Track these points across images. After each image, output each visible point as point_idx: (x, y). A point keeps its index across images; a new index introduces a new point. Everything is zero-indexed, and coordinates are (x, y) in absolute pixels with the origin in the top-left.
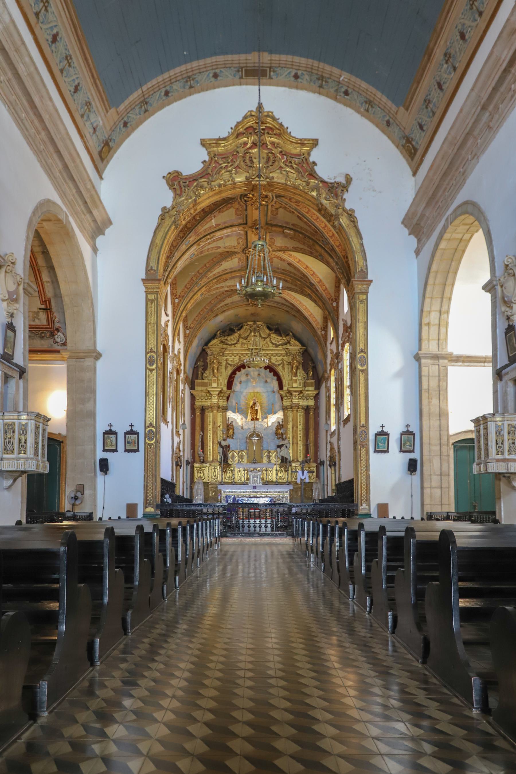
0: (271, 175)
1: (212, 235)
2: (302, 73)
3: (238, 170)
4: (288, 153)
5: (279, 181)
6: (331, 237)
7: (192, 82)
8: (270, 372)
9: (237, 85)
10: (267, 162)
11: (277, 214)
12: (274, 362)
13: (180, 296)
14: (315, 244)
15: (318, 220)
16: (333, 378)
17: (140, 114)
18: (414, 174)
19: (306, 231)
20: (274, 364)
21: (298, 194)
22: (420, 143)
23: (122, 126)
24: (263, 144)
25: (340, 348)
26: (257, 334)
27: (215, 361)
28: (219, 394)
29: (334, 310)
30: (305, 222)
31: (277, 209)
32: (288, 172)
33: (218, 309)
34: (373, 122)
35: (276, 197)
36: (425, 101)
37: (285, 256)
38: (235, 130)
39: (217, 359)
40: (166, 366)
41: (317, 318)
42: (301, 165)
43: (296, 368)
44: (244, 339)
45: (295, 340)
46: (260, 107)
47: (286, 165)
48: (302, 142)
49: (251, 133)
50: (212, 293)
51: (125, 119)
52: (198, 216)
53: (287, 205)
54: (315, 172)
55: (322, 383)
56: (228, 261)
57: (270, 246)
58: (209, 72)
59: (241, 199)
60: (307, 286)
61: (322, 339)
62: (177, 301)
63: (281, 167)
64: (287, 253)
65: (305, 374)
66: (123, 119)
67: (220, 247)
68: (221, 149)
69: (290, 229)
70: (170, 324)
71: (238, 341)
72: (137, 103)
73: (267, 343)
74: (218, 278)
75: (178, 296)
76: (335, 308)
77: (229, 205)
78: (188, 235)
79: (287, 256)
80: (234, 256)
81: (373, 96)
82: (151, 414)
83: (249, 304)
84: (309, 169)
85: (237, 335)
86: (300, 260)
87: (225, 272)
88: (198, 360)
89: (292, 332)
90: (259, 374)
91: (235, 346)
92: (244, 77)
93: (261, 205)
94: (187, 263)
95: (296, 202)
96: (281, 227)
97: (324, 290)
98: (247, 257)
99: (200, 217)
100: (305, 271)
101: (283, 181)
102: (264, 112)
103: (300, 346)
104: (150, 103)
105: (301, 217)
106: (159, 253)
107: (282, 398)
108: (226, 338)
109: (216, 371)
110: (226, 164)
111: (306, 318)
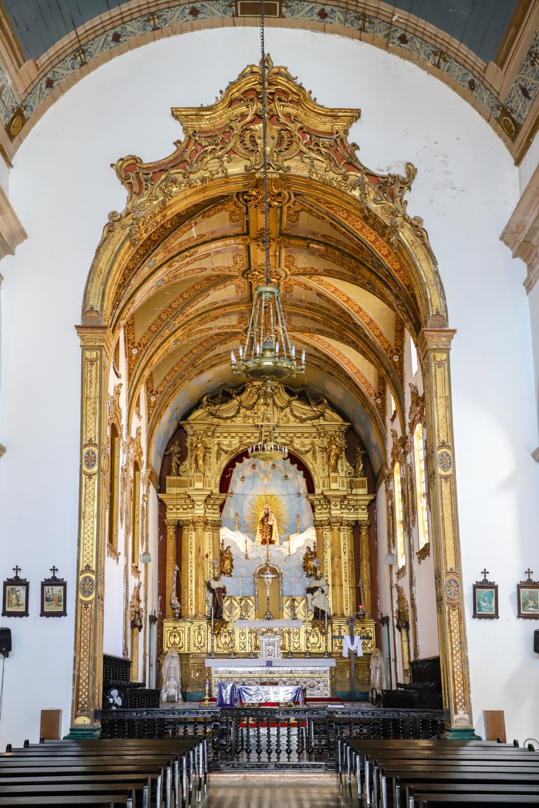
0: (286, 164)
1: (192, 251)
2: (332, 9)
3: (232, 156)
4: (313, 130)
5: (298, 173)
7: (157, 21)
8: (292, 463)
9: (229, 25)
10: (279, 144)
11: (297, 219)
12: (298, 446)
13: (139, 344)
14: (360, 266)
16: (397, 477)
17: (74, 69)
18: (518, 162)
19: (346, 246)
20: (298, 450)
21: (330, 194)
22: (524, 116)
23: (44, 86)
24: (272, 116)
25: (408, 429)
26: (270, 401)
27: (199, 446)
28: (206, 501)
29: (396, 368)
30: (344, 234)
32: (312, 160)
33: (204, 362)
34: (447, 83)
35: (295, 195)
36: (530, 54)
37: (312, 282)
38: (227, 95)
39: (203, 442)
40: (116, 458)
41: (368, 378)
42: (335, 148)
43: (335, 458)
44: (247, 409)
45: (333, 411)
46: (265, 60)
47: (309, 148)
48: (335, 114)
49: (252, 100)
50: (194, 338)
51: (50, 76)
53: (313, 207)
54: (357, 159)
55: (380, 484)
56: (219, 289)
57: (286, 267)
58: (183, 6)
59: (238, 198)
60: (350, 329)
61: (377, 412)
62: (135, 351)
63: (301, 151)
64: (314, 278)
65: (351, 468)
66: (45, 76)
67: (206, 269)
68: (204, 124)
69: (319, 242)
70: (124, 391)
71: (238, 412)
72: (68, 52)
73: (286, 416)
74: (203, 316)
75: (136, 345)
76: (397, 365)
77: (220, 207)
78: (153, 252)
79: (315, 283)
80: (229, 283)
81: (446, 44)
82: (88, 550)
84: (347, 156)
85: (235, 402)
86: (336, 289)
87: (214, 306)
88: (171, 443)
89: (326, 398)
90: (274, 465)
91: (232, 421)
92: (239, 15)
93: (270, 206)
94: (151, 293)
96: (304, 239)
97: (377, 336)
98: (251, 282)
100: (345, 306)
101: (305, 174)
102: (273, 67)
103: (340, 421)
104: (91, 52)
105: (335, 225)
106: (105, 284)
107: (313, 507)
108: (217, 407)
109: (200, 462)
110: (213, 147)
111: (349, 378)
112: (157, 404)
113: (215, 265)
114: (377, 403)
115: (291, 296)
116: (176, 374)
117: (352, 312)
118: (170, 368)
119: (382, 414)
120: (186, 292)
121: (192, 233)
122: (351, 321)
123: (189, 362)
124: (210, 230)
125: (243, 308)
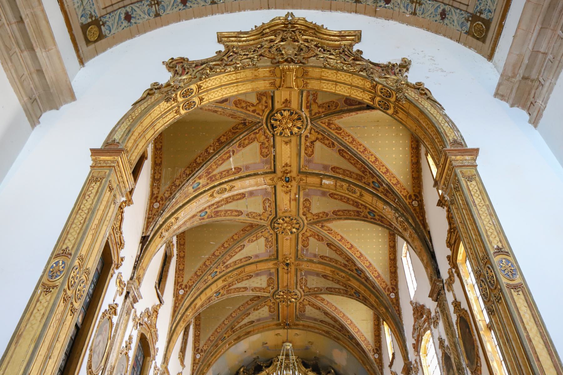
6: (385, 173)
15: (366, 153)
29: (393, 304)
31: (312, 143)
52: (212, 148)
56: (252, 241)
60: (354, 277)
61: (376, 365)
69: (329, 177)
74: (240, 270)
76: (395, 301)
79: (326, 232)
83: (280, 324)
86: (342, 237)
89: (333, 369)
95: (337, 129)
96: (318, 175)
97: (376, 277)
99: (214, 150)
100: (350, 252)
112: (201, 360)
113: (250, 210)
114: (375, 358)
115: (307, 250)
116: (219, 335)
117: (355, 258)
118: (214, 330)
119: (380, 368)
120: (227, 242)
121: (230, 164)
122: (354, 268)
123: (229, 324)
124: (245, 163)
125: (270, 265)
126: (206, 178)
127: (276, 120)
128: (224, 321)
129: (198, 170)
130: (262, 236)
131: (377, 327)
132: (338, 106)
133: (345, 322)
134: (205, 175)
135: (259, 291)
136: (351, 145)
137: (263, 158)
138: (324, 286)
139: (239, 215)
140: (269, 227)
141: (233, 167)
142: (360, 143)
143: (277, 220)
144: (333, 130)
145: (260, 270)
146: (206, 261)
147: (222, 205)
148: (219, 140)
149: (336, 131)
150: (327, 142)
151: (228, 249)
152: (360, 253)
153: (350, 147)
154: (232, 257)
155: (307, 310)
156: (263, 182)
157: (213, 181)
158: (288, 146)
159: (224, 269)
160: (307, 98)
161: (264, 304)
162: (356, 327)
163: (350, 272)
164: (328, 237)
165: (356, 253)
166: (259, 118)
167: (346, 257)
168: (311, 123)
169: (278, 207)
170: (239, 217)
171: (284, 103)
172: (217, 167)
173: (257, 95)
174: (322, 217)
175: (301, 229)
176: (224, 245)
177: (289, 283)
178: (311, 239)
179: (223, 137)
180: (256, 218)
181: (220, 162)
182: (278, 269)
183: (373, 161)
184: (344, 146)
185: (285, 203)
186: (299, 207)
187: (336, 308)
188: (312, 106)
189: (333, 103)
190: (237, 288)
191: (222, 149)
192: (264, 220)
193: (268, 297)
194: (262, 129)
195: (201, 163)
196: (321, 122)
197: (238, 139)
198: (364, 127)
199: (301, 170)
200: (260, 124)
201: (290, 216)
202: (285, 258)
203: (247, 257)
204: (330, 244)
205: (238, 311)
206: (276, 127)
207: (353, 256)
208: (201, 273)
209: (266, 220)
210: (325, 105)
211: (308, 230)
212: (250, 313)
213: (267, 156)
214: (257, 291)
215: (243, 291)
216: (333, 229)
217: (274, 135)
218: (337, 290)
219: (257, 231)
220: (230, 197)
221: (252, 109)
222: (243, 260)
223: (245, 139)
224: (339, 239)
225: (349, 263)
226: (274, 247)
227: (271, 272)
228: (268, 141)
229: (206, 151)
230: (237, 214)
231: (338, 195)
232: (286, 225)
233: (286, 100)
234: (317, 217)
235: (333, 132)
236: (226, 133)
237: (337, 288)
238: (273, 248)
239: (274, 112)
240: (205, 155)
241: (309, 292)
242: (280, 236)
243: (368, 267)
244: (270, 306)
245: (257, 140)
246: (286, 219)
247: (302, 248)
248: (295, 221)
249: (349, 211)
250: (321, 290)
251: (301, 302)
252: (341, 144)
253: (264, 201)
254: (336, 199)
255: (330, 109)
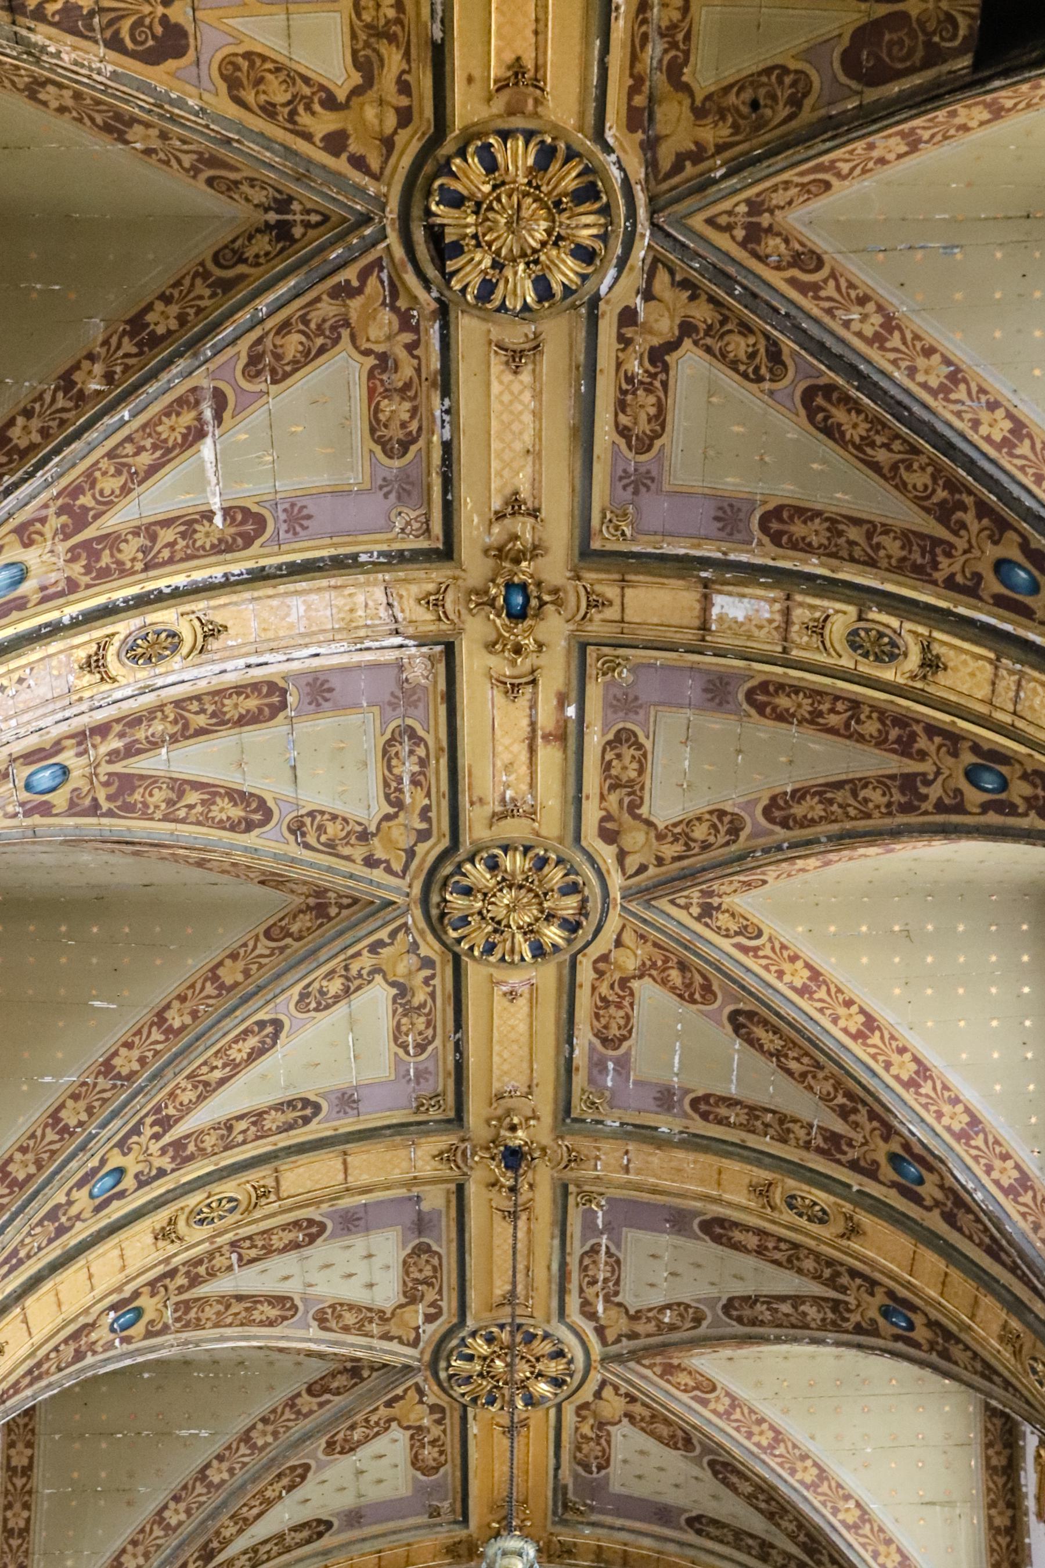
31: (658, 356)
52: (98, 369)
74: (255, 1175)
79: (726, 944)
86: (816, 975)
95: (797, 260)
97: (1007, 1191)
99: (109, 378)
115: (623, 1065)
120: (182, 999)
121: (199, 482)
122: (880, 1151)
124: (287, 485)
126: (62, 548)
127: (456, 201)
128: (165, 1507)
129: (16, 486)
130: (376, 970)
131: (1004, 1541)
132: (805, 95)
133: (827, 1513)
134: (55, 522)
135: (360, 1329)
136: (873, 353)
137: (386, 461)
138: (713, 1292)
139: (250, 826)
140: (415, 917)
141: (216, 504)
142: (928, 341)
143: (458, 870)
144: (778, 268)
145: (367, 1190)
146: (62, 1106)
147: (154, 744)
148: (136, 324)
149: (795, 272)
150: (739, 346)
151: (186, 1039)
152: (916, 1059)
153: (869, 362)
154: (207, 1089)
155: (617, 1455)
156: (383, 612)
157: (104, 574)
158: (526, 377)
159: (165, 1162)
160: (634, 58)
161: (384, 1412)
162: (889, 1542)
163: (856, 1182)
164: (738, 973)
165: (895, 1058)
166: (362, 191)
167: (838, 1085)
168: (654, 225)
169: (464, 783)
170: (250, 839)
171: (502, 86)
172: (125, 490)
173: (354, 36)
174: (706, 846)
175: (589, 926)
176: (169, 1015)
177: (520, 1277)
178: (646, 989)
179: (159, 306)
180: (346, 851)
181: (145, 459)
182: (460, 1189)
183: (997, 437)
184: (837, 362)
185: (504, 757)
186: (580, 790)
187: (778, 1437)
188: (659, 112)
189: (780, 81)
190: (240, 1298)
191: (153, 375)
192: (389, 870)
193: (407, 1369)
194: (378, 264)
195: (33, 447)
196: (710, 222)
197: (244, 316)
198: (949, 247)
199: (596, 545)
200: (368, 232)
201: (529, 838)
202: (499, 1119)
203: (291, 1104)
204: (751, 1015)
205: (244, 1450)
206: (457, 249)
207: (875, 1074)
208: (32, 1169)
209: (397, 867)
210: (732, 99)
211: (628, 938)
212: (307, 1467)
213: (405, 446)
214: (346, 1329)
215: (271, 1323)
216: (770, 925)
217: (443, 312)
218: (786, 1308)
219: (348, 938)
220: (198, 698)
221: (323, 123)
222: (271, 1122)
223: (285, 327)
224: (798, 984)
225: (856, 1125)
226: (441, 1047)
227: (425, 1206)
228: (411, 347)
229: (66, 382)
230: (236, 813)
231: (796, 690)
232: (507, 897)
233: (517, 68)
234: (678, 848)
235: (776, 278)
236: (178, 284)
237: (783, 1299)
238: (435, 1055)
239: (448, 147)
240: (61, 403)
241: (633, 1336)
242: (475, 974)
243: (962, 1136)
244: (420, 1429)
245: (353, 338)
246: (514, 863)
247: (592, 1049)
248: (555, 876)
249: (855, 786)
250: (698, 1320)
251: (585, 1406)
252: (820, 350)
253: (389, 743)
254: (782, 717)
255: (759, 126)
